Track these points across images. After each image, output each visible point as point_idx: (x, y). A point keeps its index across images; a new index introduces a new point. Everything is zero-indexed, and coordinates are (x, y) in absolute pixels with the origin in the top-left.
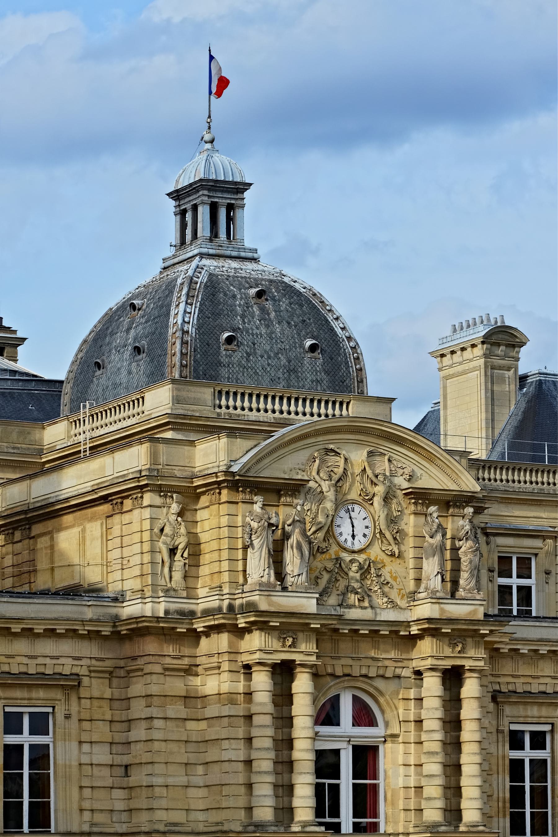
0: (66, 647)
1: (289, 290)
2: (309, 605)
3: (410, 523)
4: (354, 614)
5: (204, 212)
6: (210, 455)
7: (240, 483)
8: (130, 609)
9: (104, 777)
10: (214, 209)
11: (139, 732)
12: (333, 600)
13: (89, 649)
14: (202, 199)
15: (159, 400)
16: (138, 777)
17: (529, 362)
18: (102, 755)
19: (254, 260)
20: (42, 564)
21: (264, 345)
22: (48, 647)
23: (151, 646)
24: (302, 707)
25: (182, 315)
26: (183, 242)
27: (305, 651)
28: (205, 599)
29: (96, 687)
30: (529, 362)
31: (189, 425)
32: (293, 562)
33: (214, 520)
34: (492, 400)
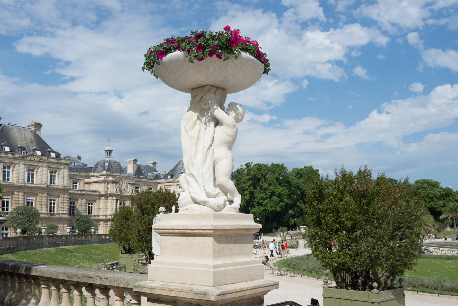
0: (95, 197)
1: (117, 162)
2: (119, 194)
3: (129, 186)
6: (110, 179)
7: (113, 182)
14: (108, 152)
15: (104, 173)
20: (91, 187)
22: (93, 197)
25: (107, 164)
27: (119, 198)
28: (109, 192)
31: (107, 176)
32: (118, 189)
33: (110, 185)
34: (134, 167)
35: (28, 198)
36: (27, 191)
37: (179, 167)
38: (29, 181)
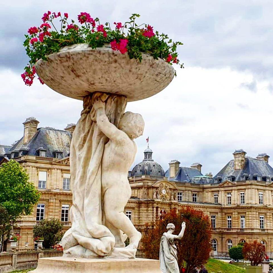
0: (133, 204)
2: (159, 200)
4: (164, 201)
5: (148, 155)
8: (141, 200)
9: (137, 219)
10: (149, 155)
11: (141, 214)
12: (162, 200)
13: (135, 204)
16: (140, 219)
17: (180, 166)
18: (137, 216)
19: (153, 161)
21: (154, 171)
23: (143, 205)
24: (159, 211)
26: (145, 158)
29: (137, 209)
30: (180, 166)
34: (176, 170)
35: (63, 206)
36: (62, 198)
37: (226, 170)
38: (64, 187)
